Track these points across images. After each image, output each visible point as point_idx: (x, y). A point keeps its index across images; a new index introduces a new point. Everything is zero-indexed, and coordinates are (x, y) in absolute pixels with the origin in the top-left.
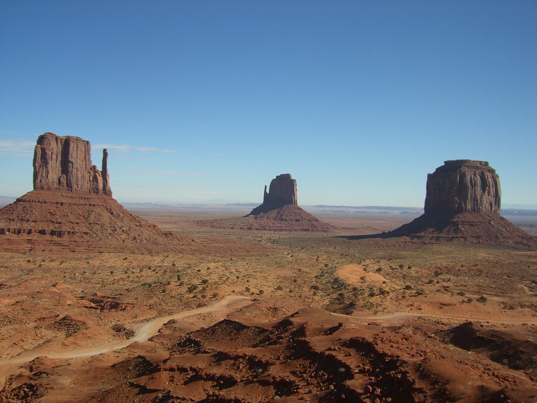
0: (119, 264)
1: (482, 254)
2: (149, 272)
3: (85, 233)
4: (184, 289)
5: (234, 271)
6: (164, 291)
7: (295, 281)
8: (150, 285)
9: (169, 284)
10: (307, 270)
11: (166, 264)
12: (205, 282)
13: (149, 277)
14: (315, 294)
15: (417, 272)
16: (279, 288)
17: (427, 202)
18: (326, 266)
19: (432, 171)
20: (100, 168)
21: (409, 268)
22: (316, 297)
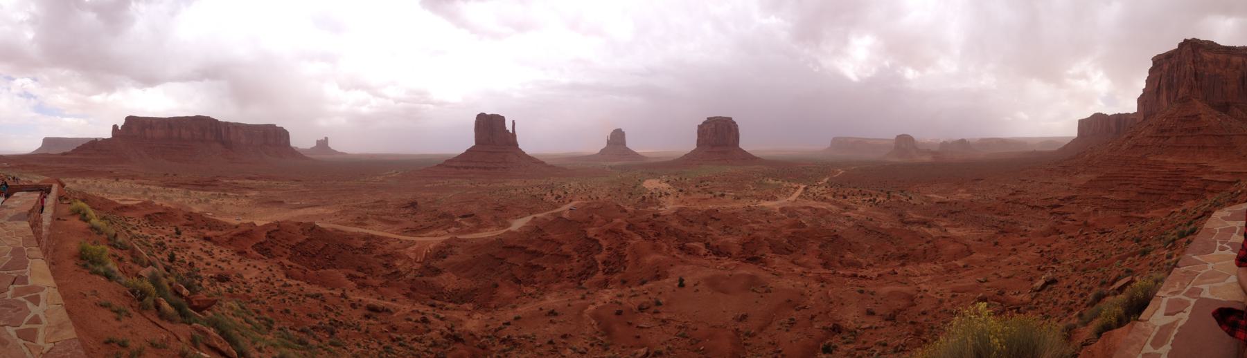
0: (521, 185)
1: (729, 169)
2: (538, 189)
3: (504, 168)
4: (554, 197)
5: (584, 186)
6: (542, 199)
7: (620, 190)
8: (535, 196)
9: (545, 195)
10: (628, 184)
11: (548, 183)
12: (566, 193)
13: (536, 191)
14: (629, 197)
15: (689, 181)
16: (609, 195)
17: (698, 141)
18: (640, 180)
19: (701, 123)
20: (511, 131)
21: (686, 179)
22: (630, 200)
